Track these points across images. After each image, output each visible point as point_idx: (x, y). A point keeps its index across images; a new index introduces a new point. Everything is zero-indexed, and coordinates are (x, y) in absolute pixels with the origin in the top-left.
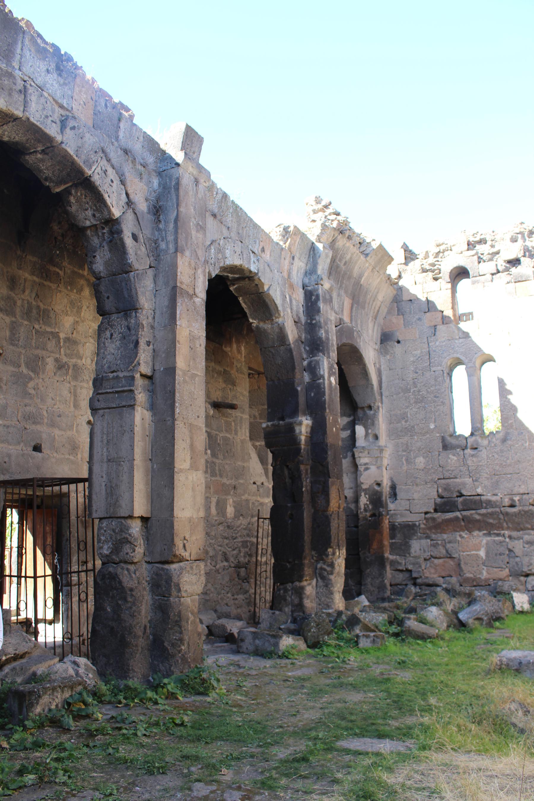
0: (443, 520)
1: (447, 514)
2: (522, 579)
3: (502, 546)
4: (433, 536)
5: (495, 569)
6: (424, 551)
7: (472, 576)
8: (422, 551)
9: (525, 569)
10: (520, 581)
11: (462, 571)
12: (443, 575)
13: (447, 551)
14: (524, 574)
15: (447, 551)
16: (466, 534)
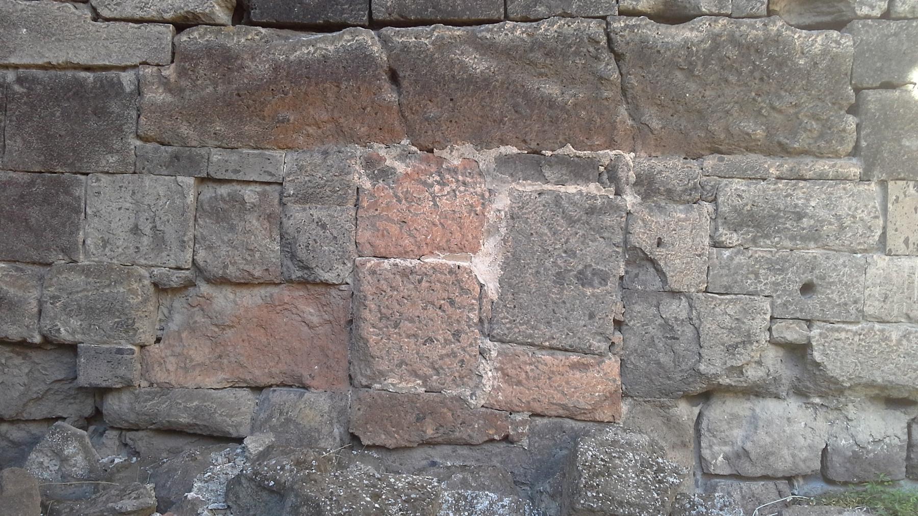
0: (276, 68)
1: (305, 37)
2: (685, 411)
3: (600, 230)
4: (217, 159)
5: (546, 357)
6: (159, 241)
7: (416, 387)
8: (145, 240)
9: (713, 365)
10: (670, 423)
11: (367, 358)
12: (260, 376)
13: (288, 245)
14: (699, 387)
15: (288, 245)
16: (405, 156)
